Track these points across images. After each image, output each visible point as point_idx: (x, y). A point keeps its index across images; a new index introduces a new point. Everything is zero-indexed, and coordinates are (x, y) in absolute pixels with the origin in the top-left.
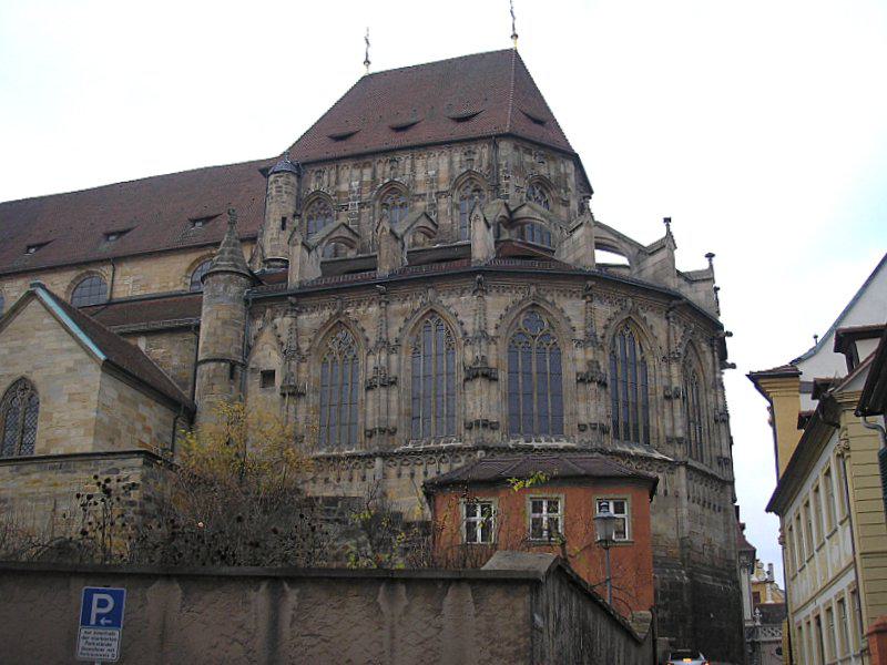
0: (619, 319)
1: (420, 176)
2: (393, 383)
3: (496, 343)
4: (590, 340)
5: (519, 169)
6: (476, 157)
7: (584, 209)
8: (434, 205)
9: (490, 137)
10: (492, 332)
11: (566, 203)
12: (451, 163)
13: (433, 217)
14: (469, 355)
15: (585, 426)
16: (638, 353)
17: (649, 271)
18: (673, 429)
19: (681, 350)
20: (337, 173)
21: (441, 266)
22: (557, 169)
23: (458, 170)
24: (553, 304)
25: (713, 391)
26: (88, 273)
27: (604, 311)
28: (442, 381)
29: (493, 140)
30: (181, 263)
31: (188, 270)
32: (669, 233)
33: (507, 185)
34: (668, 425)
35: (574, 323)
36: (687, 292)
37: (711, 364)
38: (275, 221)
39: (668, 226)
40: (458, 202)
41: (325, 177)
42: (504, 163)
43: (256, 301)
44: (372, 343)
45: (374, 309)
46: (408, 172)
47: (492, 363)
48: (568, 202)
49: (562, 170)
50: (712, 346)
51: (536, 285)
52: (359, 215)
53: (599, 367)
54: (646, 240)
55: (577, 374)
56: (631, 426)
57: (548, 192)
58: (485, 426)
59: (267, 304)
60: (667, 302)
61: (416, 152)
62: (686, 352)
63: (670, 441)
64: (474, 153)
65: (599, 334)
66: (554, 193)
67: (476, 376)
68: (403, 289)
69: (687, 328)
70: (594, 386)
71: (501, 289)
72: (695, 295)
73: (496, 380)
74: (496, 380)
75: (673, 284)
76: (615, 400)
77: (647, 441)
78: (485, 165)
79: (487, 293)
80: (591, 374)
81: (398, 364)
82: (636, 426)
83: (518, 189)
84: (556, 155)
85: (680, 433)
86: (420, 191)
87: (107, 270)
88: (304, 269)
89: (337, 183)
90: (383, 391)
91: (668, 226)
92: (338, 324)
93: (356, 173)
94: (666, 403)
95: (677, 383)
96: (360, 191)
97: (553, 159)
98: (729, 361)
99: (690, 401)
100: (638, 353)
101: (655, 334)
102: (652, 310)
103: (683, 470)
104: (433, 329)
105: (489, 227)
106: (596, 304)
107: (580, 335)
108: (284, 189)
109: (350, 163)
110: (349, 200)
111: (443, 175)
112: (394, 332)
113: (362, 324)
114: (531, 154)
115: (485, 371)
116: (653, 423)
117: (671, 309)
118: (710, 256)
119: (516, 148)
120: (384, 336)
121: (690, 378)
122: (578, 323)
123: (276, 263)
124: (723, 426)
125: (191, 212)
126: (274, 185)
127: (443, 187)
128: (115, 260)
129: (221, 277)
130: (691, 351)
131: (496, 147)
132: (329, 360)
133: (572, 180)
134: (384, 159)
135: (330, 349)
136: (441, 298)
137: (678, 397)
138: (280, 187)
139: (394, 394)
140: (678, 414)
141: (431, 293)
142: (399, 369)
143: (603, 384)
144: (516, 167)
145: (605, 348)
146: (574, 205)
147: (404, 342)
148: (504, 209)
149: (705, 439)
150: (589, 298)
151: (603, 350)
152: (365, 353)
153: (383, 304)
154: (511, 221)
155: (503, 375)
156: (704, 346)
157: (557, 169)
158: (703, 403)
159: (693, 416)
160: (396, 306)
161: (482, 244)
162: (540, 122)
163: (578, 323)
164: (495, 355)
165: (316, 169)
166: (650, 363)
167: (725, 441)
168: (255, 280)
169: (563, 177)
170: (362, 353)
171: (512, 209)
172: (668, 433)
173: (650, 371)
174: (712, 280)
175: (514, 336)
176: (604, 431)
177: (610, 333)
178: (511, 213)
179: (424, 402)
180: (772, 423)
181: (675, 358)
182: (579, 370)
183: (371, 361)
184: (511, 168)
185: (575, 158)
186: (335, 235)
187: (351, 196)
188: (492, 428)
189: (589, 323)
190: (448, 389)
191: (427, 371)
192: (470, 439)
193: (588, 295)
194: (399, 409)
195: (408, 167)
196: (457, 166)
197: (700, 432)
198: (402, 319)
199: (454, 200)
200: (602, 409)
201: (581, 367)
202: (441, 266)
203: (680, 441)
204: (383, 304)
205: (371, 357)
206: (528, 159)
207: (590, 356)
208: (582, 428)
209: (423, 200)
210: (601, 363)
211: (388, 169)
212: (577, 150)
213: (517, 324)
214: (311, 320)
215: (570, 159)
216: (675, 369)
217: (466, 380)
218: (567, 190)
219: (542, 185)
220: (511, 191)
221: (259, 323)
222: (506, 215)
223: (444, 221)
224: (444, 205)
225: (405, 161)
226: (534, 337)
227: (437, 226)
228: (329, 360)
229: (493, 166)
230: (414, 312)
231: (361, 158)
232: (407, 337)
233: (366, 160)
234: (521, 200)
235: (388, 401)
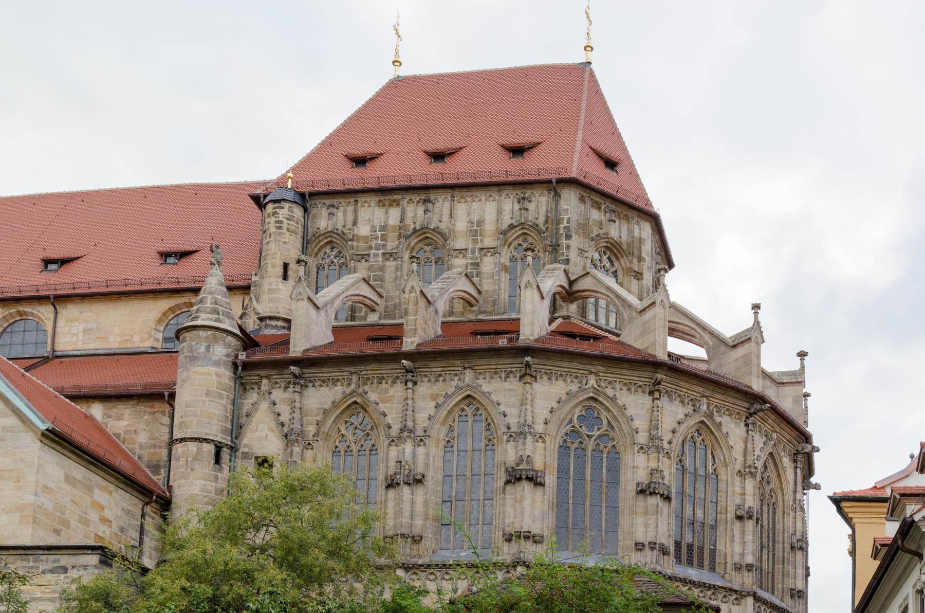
0: (692, 422)
1: (461, 225)
2: (419, 482)
3: (544, 442)
4: (654, 445)
5: (584, 227)
6: (532, 207)
7: (657, 284)
8: (478, 264)
9: (550, 182)
10: (539, 428)
11: (638, 276)
12: (499, 212)
13: (475, 280)
14: (509, 453)
15: (643, 545)
16: (710, 463)
17: (729, 368)
18: (743, 555)
19: (759, 464)
20: (355, 211)
21: (483, 343)
22: (631, 232)
23: (507, 221)
24: (613, 399)
25: (792, 514)
26: (19, 313)
27: (673, 413)
28: (479, 483)
29: (556, 185)
30: (154, 309)
31: (159, 321)
32: (757, 323)
33: (568, 247)
34: (737, 549)
35: (637, 423)
36: (771, 393)
37: (792, 482)
38: (274, 266)
39: (756, 313)
40: (508, 263)
41: (340, 215)
42: (566, 217)
43: (247, 366)
44: (395, 431)
45: (397, 391)
46: (446, 218)
47: (538, 465)
48: (641, 274)
49: (636, 234)
50: (795, 461)
51: (596, 374)
52: (382, 269)
53: (663, 478)
54: (729, 329)
55: (638, 484)
56: (695, 548)
57: (618, 259)
58: (527, 538)
59: (263, 373)
60: (747, 405)
61: (457, 194)
62: (765, 467)
63: (738, 568)
64: (530, 202)
65: (666, 438)
66: (624, 262)
67: (519, 479)
68: (436, 367)
69: (768, 437)
70: (654, 500)
71: (554, 378)
72: (785, 401)
73: (542, 485)
74: (542, 485)
75: (757, 385)
76: (681, 517)
77: (713, 569)
78: (541, 220)
79: (536, 381)
80: (653, 486)
81: (427, 458)
82: (701, 549)
83: (582, 251)
84: (630, 213)
85: (749, 559)
86: (460, 244)
87: (45, 312)
88: (311, 333)
89: (355, 223)
90: (406, 490)
91: (756, 313)
92: (355, 406)
94: (737, 524)
95: (751, 502)
96: (384, 238)
97: (627, 218)
98: (813, 480)
99: (765, 523)
100: (710, 463)
101: (731, 443)
102: (730, 415)
103: (750, 600)
104: (470, 418)
105: (543, 298)
106: (664, 402)
107: (642, 438)
108: (285, 226)
109: (373, 199)
110: (370, 248)
111: (489, 226)
112: (422, 418)
113: (382, 407)
114: (599, 208)
115: (530, 474)
116: (720, 547)
117: (751, 415)
118: (802, 355)
119: (582, 199)
120: (410, 424)
121: (767, 499)
122: (641, 423)
123: (274, 323)
124: (799, 554)
125: (170, 245)
126: (273, 219)
127: (489, 242)
128: (58, 300)
129: (203, 334)
130: (771, 466)
131: (557, 195)
132: (342, 447)
133: (648, 247)
134: (416, 197)
135: (343, 436)
136: (480, 382)
137: (750, 517)
138: (281, 222)
139: (420, 491)
140: (749, 537)
141: (468, 376)
142: (427, 466)
143: (667, 498)
144: (579, 225)
145: (672, 455)
146: (648, 278)
147: (433, 433)
148: (563, 276)
149: (778, 567)
150: (657, 395)
151: (669, 458)
152: (387, 442)
153: (410, 385)
154: (569, 294)
155: (550, 480)
156: (786, 462)
157: (631, 232)
158: (779, 527)
159: (768, 541)
160: (424, 389)
161: (535, 323)
162: (611, 164)
163: (641, 423)
164: (543, 456)
165: (328, 202)
166: (722, 477)
167: (800, 572)
168: (248, 341)
169: (636, 245)
170: (383, 442)
171: (573, 278)
172: (737, 559)
173: (722, 486)
174: (801, 383)
175: (566, 434)
176: (665, 552)
177: (678, 439)
178: (571, 283)
179: (456, 507)
180: (853, 553)
181: (751, 473)
182: (640, 480)
183: (393, 453)
184: (573, 225)
185: (654, 220)
186: (352, 292)
187: (373, 243)
188: (535, 542)
189: (654, 425)
190: (485, 493)
191: (460, 470)
192: (507, 553)
193: (654, 391)
194: (426, 514)
195: (446, 211)
197: (773, 558)
198: (433, 404)
199: (503, 260)
200: (663, 528)
201: (642, 476)
202: (483, 343)
203: (749, 568)
204: (410, 385)
205: (393, 448)
206: (595, 215)
207: (653, 464)
208: (639, 547)
209: (464, 256)
210: (666, 473)
211: (420, 210)
212: (658, 205)
213: (571, 421)
214: (321, 397)
215: (647, 220)
216: (750, 485)
217: (508, 482)
218: (640, 259)
219: (613, 250)
220: (573, 255)
221: (253, 396)
222: (567, 286)
223: (487, 285)
224: (488, 264)
225: (442, 203)
226: (590, 437)
227: (480, 292)
228: (342, 447)
229: (554, 220)
230: (447, 396)
231: (387, 193)
232: (438, 426)
234: (584, 268)
235: (413, 502)
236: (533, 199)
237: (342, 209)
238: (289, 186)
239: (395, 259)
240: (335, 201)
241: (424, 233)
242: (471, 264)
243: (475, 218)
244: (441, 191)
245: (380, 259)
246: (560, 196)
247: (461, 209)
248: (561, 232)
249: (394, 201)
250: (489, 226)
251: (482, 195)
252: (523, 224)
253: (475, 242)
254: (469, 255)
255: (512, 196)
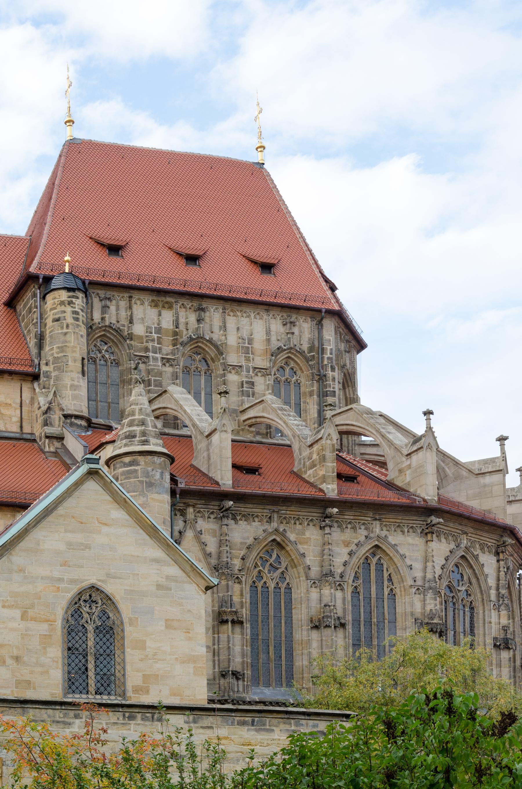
6: (296, 330)
9: (319, 311)
12: (268, 332)
23: (275, 344)
42: (329, 348)
61: (227, 305)
86: (233, 359)
93: (152, 313)
109: (147, 298)
111: (259, 345)
127: (260, 362)
131: (320, 323)
134: (188, 303)
187: (150, 345)
196: (273, 338)
209: (237, 373)
211: (192, 318)
225: (214, 315)
233: (169, 299)
236: (297, 323)
237: (114, 302)
238: (67, 271)
239: (171, 365)
240: (109, 294)
241: (197, 342)
242: (247, 382)
243: (245, 334)
244: (215, 301)
245: (160, 364)
246: (322, 326)
247: (231, 322)
248: (326, 362)
249: (167, 303)
250: (259, 345)
251: (251, 312)
252: (291, 348)
253: (248, 359)
254: (244, 373)
255: (278, 318)
